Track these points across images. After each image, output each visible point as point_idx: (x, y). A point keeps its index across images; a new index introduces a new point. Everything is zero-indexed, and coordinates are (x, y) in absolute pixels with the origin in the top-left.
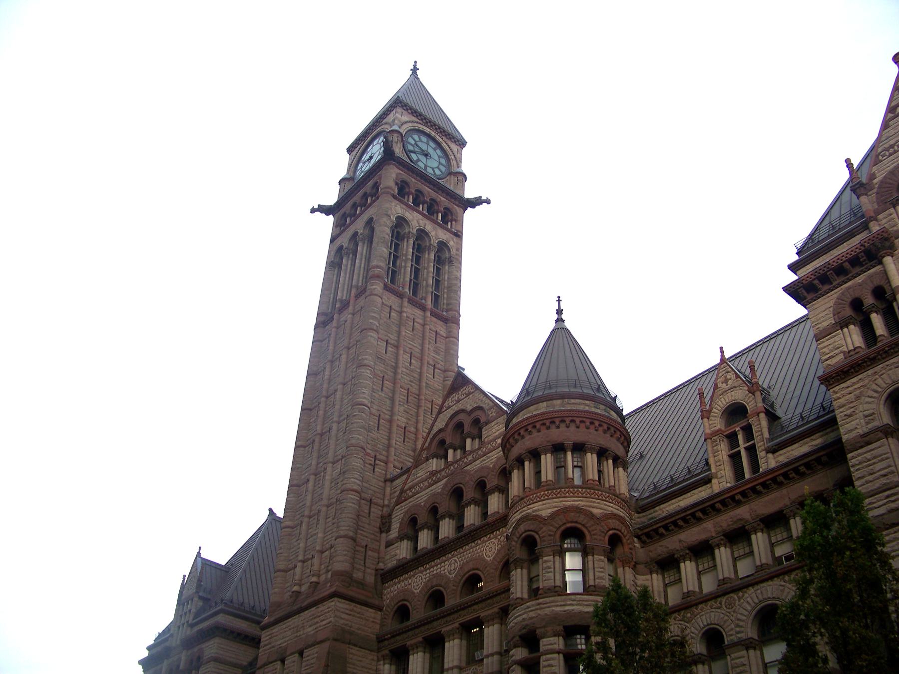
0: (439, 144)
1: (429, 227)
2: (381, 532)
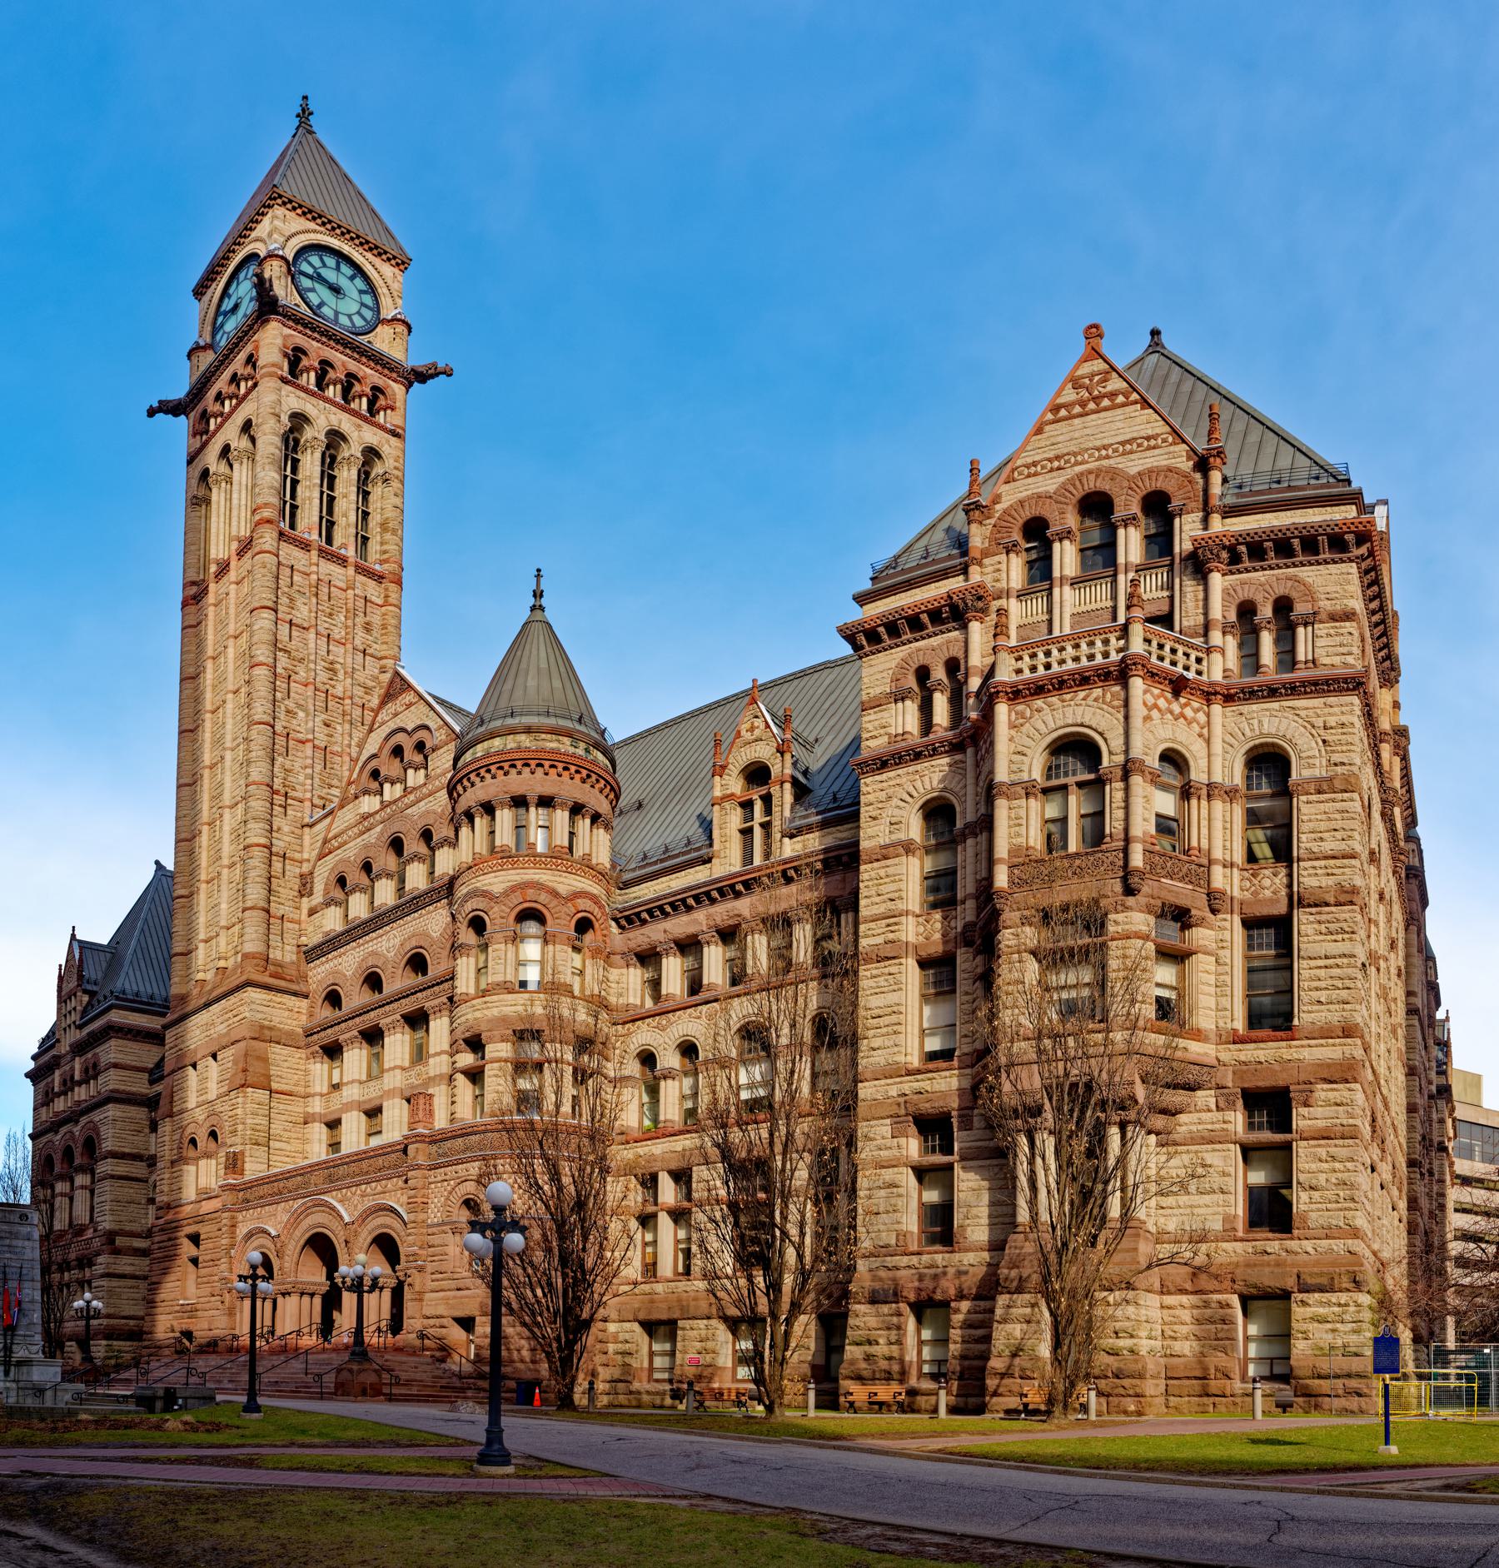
0: (359, 270)
1: (345, 423)
2: (302, 896)
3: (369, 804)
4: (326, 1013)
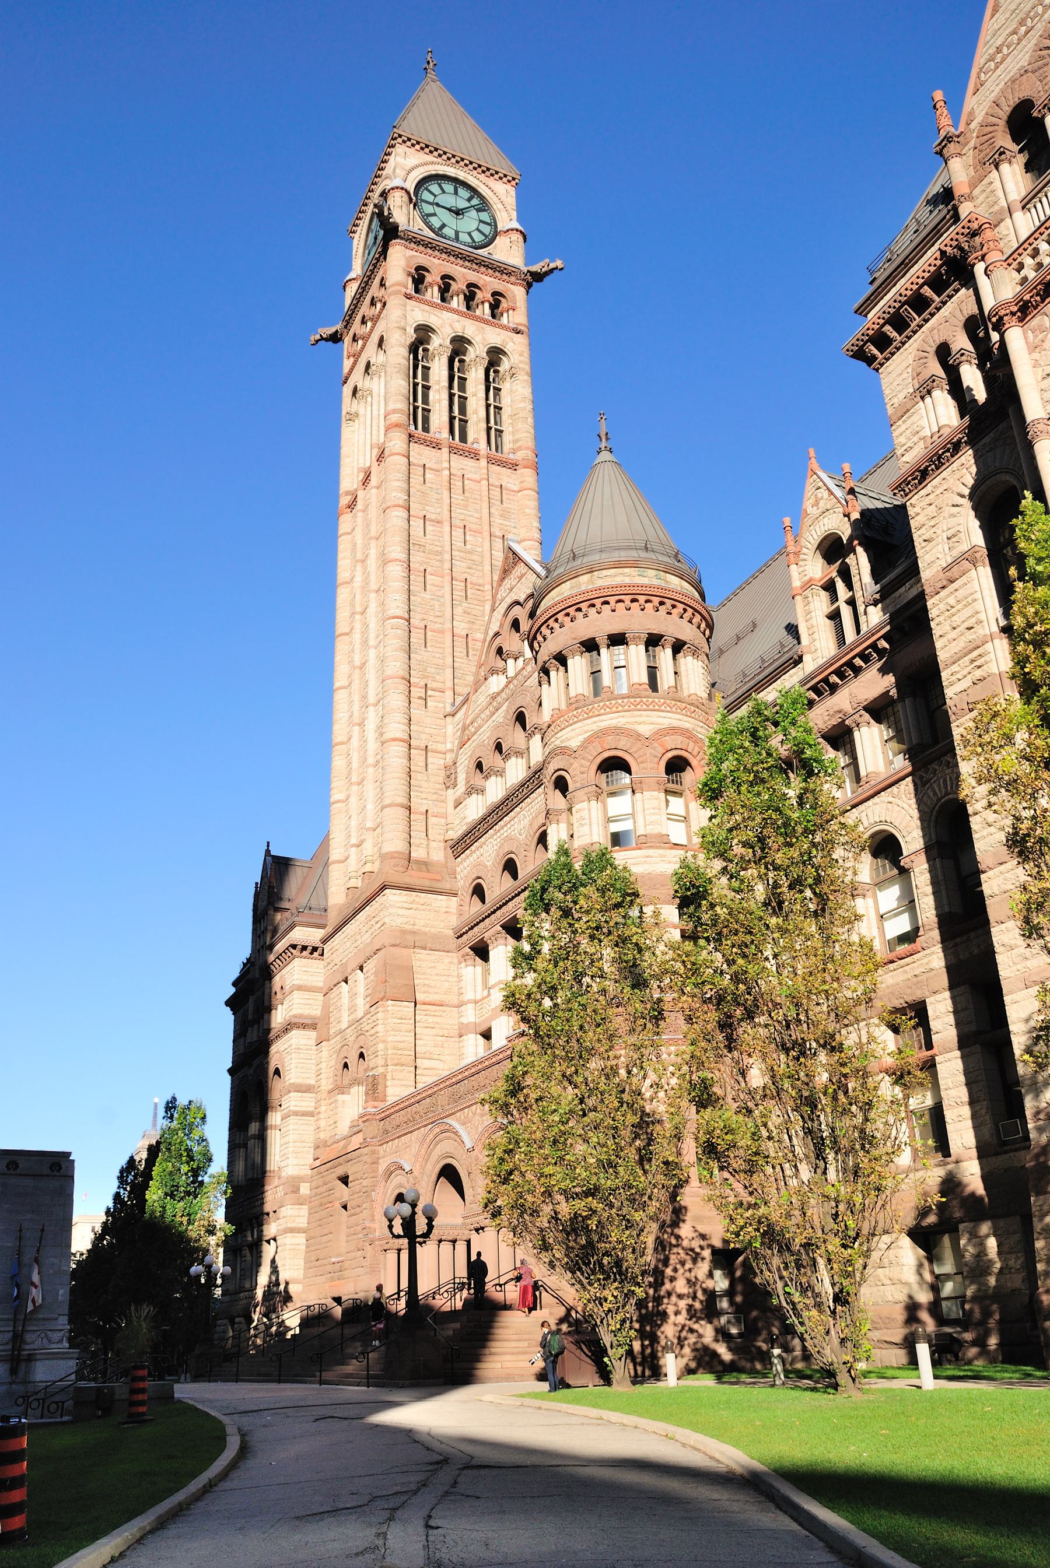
0: (474, 191)
1: (468, 328)
2: (447, 788)
3: (496, 683)
4: (476, 907)
